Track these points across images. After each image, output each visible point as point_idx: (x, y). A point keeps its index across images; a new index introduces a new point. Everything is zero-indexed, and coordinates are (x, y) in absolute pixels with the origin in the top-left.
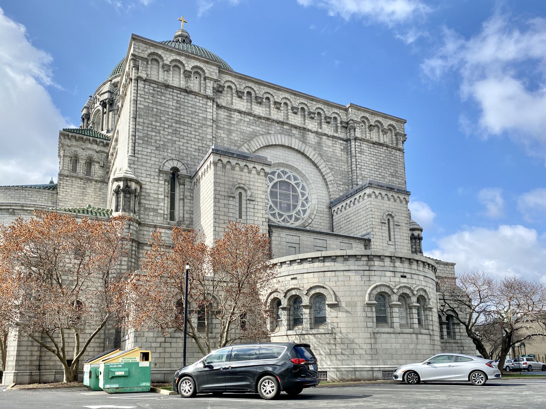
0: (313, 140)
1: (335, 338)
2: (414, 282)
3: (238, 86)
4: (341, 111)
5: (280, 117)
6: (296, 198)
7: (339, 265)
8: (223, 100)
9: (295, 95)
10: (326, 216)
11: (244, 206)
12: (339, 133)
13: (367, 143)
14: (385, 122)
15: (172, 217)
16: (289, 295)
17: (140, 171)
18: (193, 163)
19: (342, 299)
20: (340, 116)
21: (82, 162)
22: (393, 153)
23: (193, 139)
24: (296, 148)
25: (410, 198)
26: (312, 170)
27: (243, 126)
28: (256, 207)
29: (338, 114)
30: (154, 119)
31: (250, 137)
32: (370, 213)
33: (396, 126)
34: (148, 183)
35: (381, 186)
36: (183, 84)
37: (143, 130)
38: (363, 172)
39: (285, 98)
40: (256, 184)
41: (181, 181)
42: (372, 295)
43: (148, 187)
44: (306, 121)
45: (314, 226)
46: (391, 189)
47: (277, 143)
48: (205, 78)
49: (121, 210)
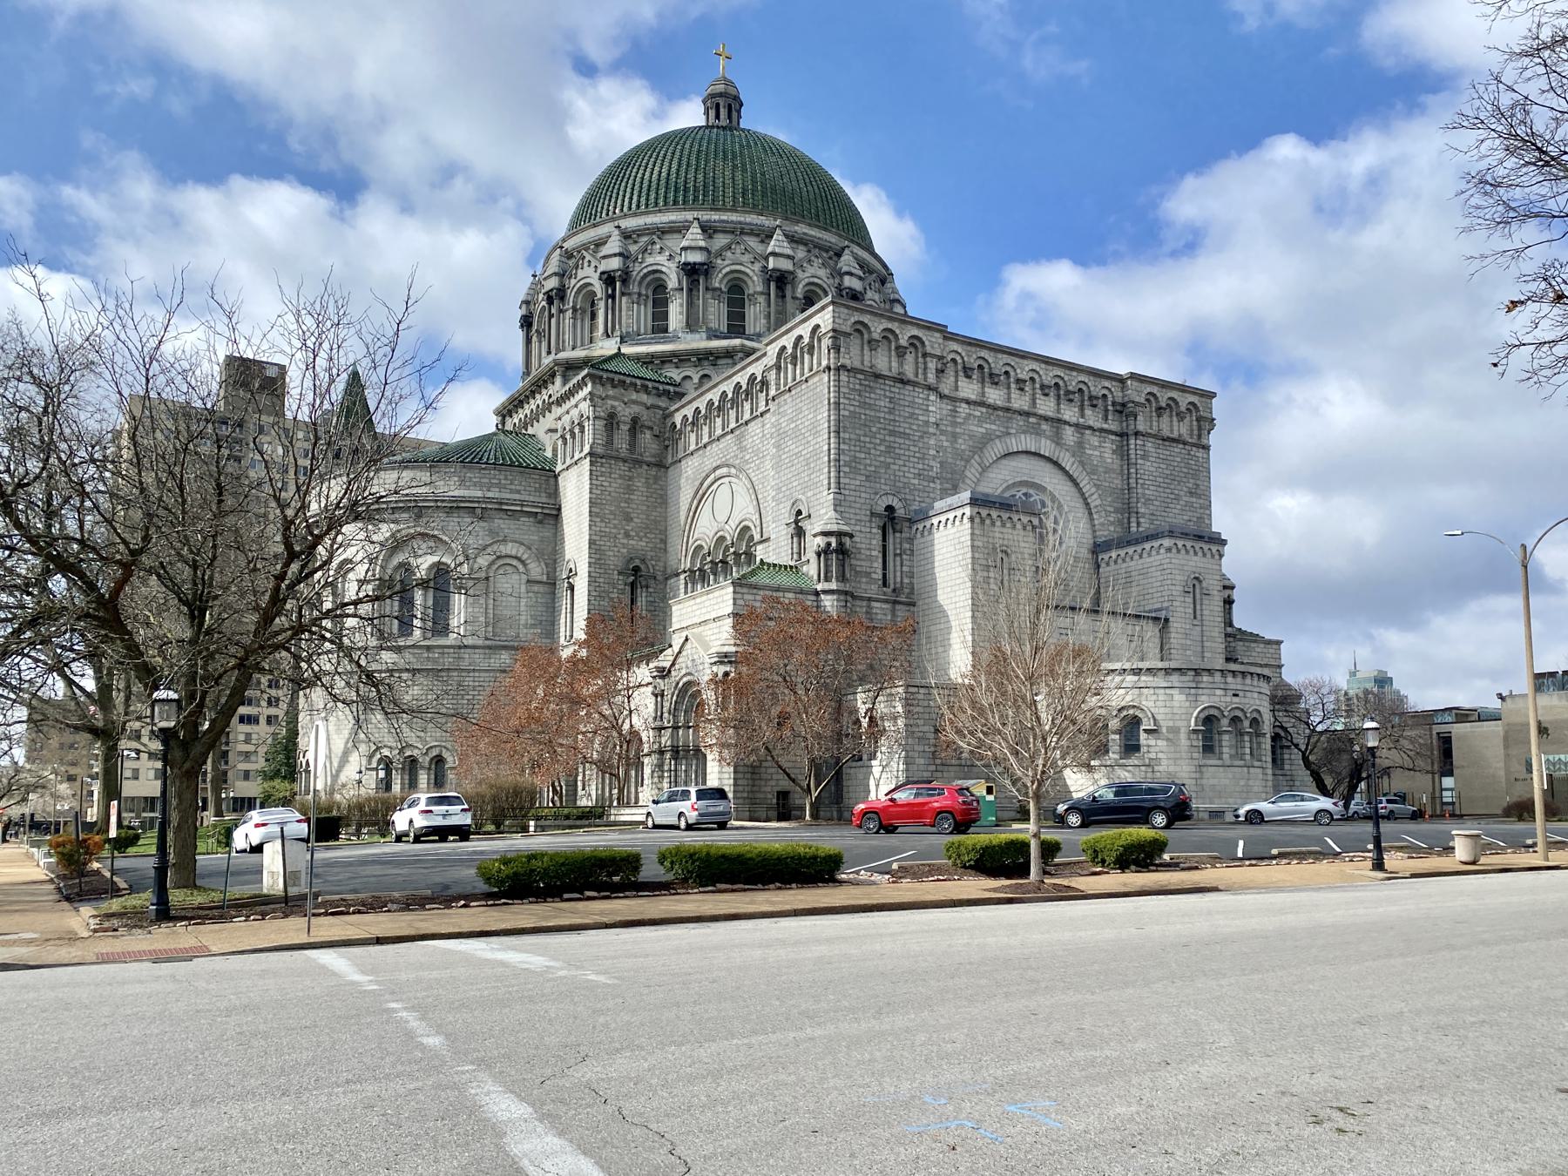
7: (1160, 681)
9: (1046, 363)
21: (625, 428)
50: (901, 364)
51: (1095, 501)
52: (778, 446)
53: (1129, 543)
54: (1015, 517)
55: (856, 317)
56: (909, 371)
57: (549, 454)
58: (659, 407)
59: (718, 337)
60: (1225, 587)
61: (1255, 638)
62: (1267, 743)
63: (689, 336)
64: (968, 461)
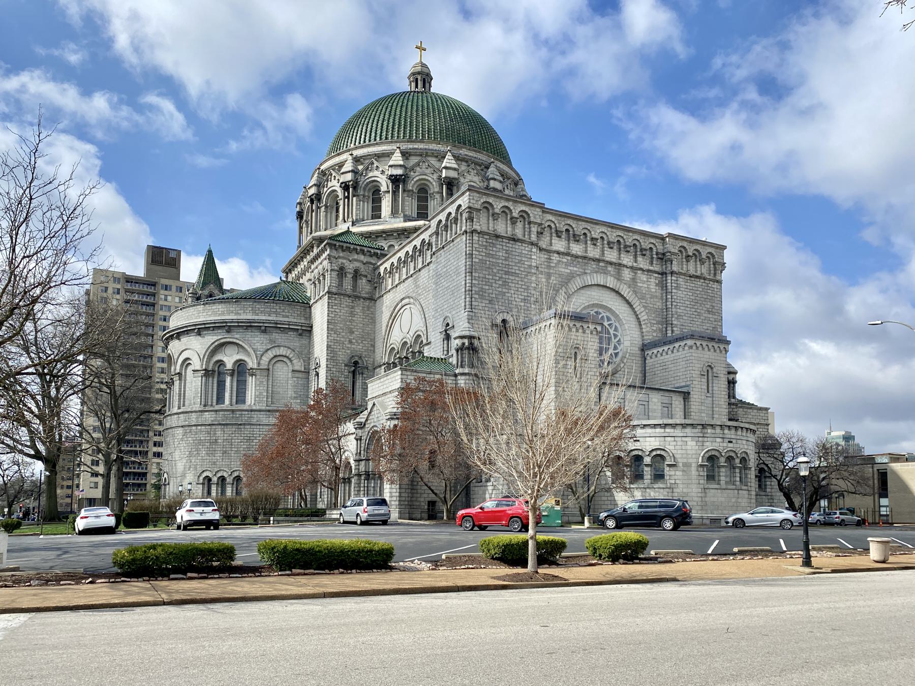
7: (678, 432)
9: (612, 227)
21: (350, 276)
50: (514, 229)
51: (643, 317)
52: (436, 283)
53: (665, 344)
54: (585, 326)
55: (484, 199)
56: (519, 232)
57: (309, 295)
58: (371, 263)
59: (410, 220)
60: (729, 373)
61: (751, 406)
62: (752, 474)
63: (393, 220)
64: (558, 291)
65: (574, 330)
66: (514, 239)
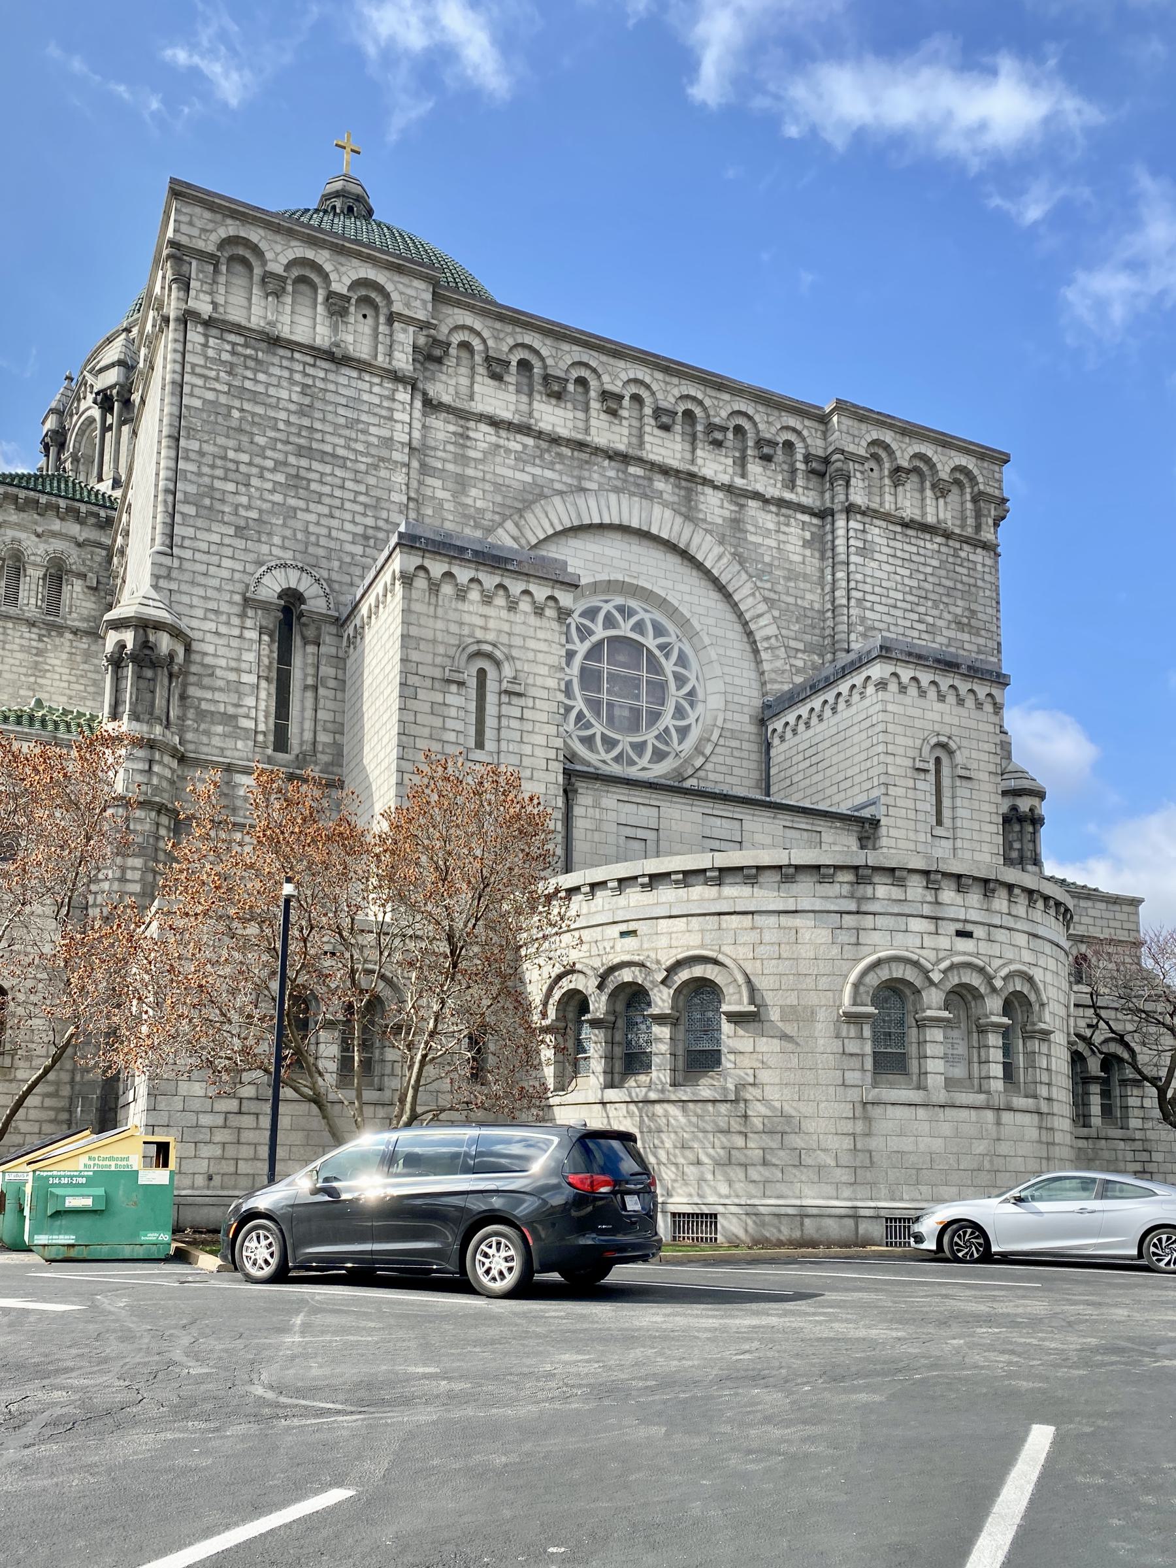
0: (717, 511)
1: (746, 1116)
2: (995, 950)
3: (490, 343)
4: (807, 423)
5: (617, 438)
6: (659, 690)
7: (766, 896)
8: (443, 389)
10: (750, 748)
11: (491, 709)
12: (800, 490)
13: (883, 524)
14: (944, 459)
15: (281, 742)
16: (610, 986)
17: (185, 599)
18: (347, 579)
19: (769, 998)
20: (804, 440)
22: (963, 554)
23: (348, 505)
24: (664, 535)
25: (1005, 696)
26: (712, 604)
27: (504, 465)
28: (528, 714)
29: (799, 433)
30: (231, 443)
31: (524, 501)
32: (881, 737)
33: (976, 472)
34: (209, 637)
35: (919, 657)
36: (322, 336)
37: (200, 474)
38: (868, 614)
39: (636, 381)
40: (531, 644)
41: (310, 633)
42: (862, 989)
43: (210, 649)
44: (699, 452)
45: (711, 776)
46: (948, 665)
47: (607, 521)
48: (391, 319)
49: (125, 717)
51: (764, 628)
65: (474, 595)
66: (336, 358)
